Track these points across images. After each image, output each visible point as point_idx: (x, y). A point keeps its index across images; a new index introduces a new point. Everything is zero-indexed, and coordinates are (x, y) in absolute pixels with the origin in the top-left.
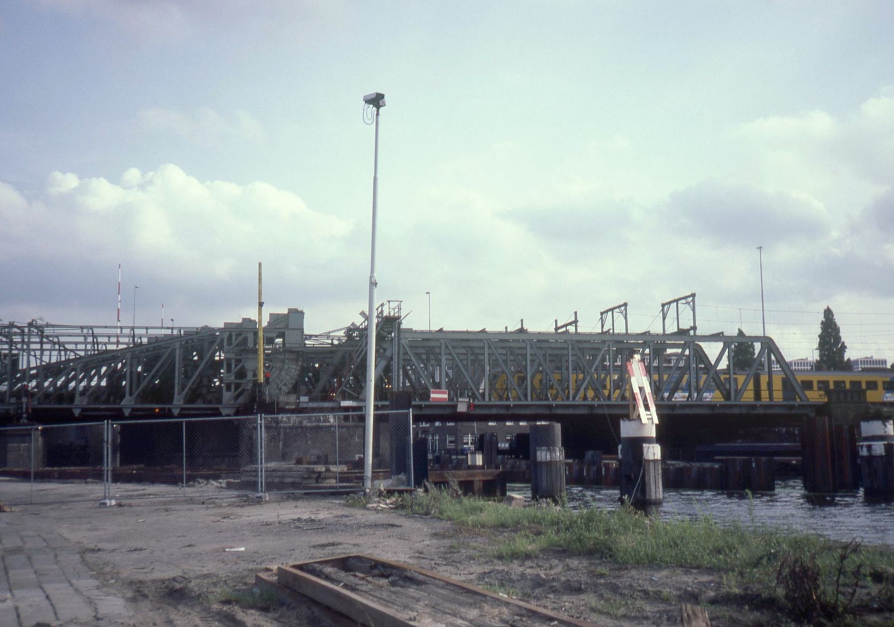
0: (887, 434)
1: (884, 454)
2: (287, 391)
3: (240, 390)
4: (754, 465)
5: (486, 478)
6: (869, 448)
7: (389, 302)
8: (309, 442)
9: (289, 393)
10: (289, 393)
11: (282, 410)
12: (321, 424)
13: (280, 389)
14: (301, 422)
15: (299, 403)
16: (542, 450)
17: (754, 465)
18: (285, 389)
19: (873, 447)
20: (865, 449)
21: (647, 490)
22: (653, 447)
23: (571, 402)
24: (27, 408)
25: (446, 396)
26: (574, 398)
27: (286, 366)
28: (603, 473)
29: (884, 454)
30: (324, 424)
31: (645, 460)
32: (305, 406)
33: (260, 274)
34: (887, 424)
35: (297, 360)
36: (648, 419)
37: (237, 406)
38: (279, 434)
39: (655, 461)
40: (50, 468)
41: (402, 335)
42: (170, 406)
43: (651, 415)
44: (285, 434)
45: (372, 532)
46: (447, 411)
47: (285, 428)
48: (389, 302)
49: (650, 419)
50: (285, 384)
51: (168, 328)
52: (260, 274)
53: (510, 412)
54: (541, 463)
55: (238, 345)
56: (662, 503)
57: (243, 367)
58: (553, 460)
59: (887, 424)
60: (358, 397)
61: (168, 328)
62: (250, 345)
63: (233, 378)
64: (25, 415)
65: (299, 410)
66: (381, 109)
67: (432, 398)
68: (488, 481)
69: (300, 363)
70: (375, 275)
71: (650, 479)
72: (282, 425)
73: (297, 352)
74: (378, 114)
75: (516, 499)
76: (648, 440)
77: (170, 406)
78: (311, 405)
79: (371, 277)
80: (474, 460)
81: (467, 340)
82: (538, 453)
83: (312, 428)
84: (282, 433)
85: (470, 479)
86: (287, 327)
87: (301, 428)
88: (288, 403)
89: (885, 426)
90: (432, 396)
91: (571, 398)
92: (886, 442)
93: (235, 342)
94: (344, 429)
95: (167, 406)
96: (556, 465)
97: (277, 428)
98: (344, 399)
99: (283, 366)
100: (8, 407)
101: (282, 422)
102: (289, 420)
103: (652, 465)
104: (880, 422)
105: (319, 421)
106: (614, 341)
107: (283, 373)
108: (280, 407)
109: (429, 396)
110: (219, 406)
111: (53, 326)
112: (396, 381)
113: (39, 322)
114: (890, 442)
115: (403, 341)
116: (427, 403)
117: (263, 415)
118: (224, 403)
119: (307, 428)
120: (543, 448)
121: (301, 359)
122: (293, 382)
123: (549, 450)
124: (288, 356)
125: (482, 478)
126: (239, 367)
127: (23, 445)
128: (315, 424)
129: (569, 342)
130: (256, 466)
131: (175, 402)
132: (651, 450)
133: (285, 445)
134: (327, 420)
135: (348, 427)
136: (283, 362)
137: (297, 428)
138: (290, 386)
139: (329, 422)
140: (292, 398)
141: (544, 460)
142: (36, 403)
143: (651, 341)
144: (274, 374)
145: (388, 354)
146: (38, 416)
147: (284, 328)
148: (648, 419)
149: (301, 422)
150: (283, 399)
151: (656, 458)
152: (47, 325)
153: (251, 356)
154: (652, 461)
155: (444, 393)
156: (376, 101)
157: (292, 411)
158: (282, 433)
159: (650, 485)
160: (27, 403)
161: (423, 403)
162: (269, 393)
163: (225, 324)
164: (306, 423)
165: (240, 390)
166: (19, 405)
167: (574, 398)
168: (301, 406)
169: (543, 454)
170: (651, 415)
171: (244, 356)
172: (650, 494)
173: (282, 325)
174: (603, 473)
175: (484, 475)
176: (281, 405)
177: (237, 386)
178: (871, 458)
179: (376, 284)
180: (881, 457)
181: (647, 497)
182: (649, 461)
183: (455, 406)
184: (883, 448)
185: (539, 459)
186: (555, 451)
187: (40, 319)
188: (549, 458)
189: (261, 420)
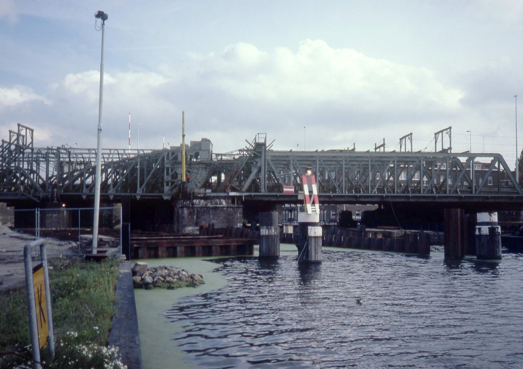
0: (491, 221)
1: (488, 234)
2: (200, 186)
3: (174, 185)
4: (418, 238)
5: (238, 244)
6: (480, 229)
7: (258, 134)
8: (211, 216)
9: (201, 187)
10: (201, 187)
11: (196, 198)
12: (218, 206)
13: (196, 185)
14: (206, 205)
15: (205, 194)
16: (263, 228)
17: (418, 238)
18: (199, 185)
19: (482, 229)
20: (477, 231)
21: (310, 255)
22: (315, 229)
23: (369, 194)
24: (57, 195)
25: (293, 190)
26: (371, 192)
27: (200, 172)
28: (342, 240)
29: (488, 234)
30: (219, 206)
31: (309, 237)
32: (209, 195)
33: (183, 118)
34: (492, 214)
35: (206, 168)
36: (312, 211)
37: (172, 194)
38: (194, 211)
39: (316, 238)
40: (74, 229)
41: (267, 154)
42: (135, 194)
43: (315, 208)
44: (197, 211)
45: (184, 273)
46: (294, 199)
47: (198, 208)
48: (258, 134)
49: (314, 211)
50: (199, 182)
51: (136, 150)
52: (183, 118)
53: (331, 200)
54: (263, 236)
55: (172, 160)
56: (321, 262)
57: (176, 172)
58: (270, 234)
59: (492, 214)
60: (241, 190)
61: (136, 150)
62: (179, 159)
63: (170, 178)
64: (55, 199)
65: (205, 198)
66: (105, 22)
67: (285, 191)
68: (241, 245)
69: (208, 170)
70: (101, 124)
71: (311, 248)
72: (195, 206)
73: (206, 164)
74: (103, 24)
75: (140, 265)
76: (314, 224)
77: (135, 194)
78: (213, 194)
79: (99, 126)
80: (287, 230)
81: (312, 157)
82: (261, 230)
83: (213, 208)
84: (196, 211)
85: (227, 244)
86: (200, 149)
87: (207, 208)
88: (199, 193)
89: (491, 216)
90: (285, 190)
91: (370, 192)
92: (490, 226)
93: (171, 158)
94: (231, 209)
95: (133, 194)
96: (272, 238)
97: (193, 208)
98: (232, 191)
99: (198, 172)
100: (47, 194)
101: (196, 204)
102: (200, 203)
103: (313, 240)
104: (487, 213)
105: (216, 204)
106: (397, 156)
107: (198, 176)
108: (195, 195)
109: (283, 190)
110: (162, 194)
111: (74, 149)
112: (263, 181)
113: (66, 147)
114: (494, 226)
115: (267, 157)
116: (281, 194)
117: (39, 209)
118: (165, 192)
119: (209, 208)
120: (264, 227)
121: (208, 168)
122: (204, 181)
123: (268, 228)
124: (201, 166)
125: (236, 244)
126: (173, 172)
127: (54, 215)
128: (215, 205)
129: (369, 158)
130: (89, 236)
131: (138, 192)
132: (313, 230)
133: (197, 218)
134: (221, 204)
135: (234, 208)
136: (198, 169)
137: (204, 208)
138: (202, 183)
139: (223, 204)
140: (202, 190)
141: (264, 234)
142: (63, 191)
143: (421, 157)
144: (192, 177)
145: (259, 165)
146: (62, 199)
147: (199, 150)
148: (312, 211)
149: (206, 205)
150: (196, 191)
151: (316, 235)
152: (70, 148)
153: (180, 166)
154: (313, 237)
155: (292, 188)
156: (101, 15)
157: (201, 198)
158: (196, 211)
159: (312, 252)
160: (57, 192)
161: (278, 194)
162: (190, 187)
163: (171, 147)
164: (209, 205)
165: (174, 185)
166: (53, 192)
167: (371, 192)
168: (207, 195)
169: (264, 230)
170: (315, 208)
171: (176, 166)
172: (311, 257)
173: (197, 148)
174: (342, 240)
175: (237, 242)
176: (195, 194)
177: (172, 183)
178: (480, 236)
179: (101, 130)
180: (486, 236)
181: (309, 259)
182: (311, 237)
183: (297, 196)
184: (488, 230)
185: (262, 234)
186: (271, 229)
187: (67, 145)
188: (267, 234)
189: (38, 211)
